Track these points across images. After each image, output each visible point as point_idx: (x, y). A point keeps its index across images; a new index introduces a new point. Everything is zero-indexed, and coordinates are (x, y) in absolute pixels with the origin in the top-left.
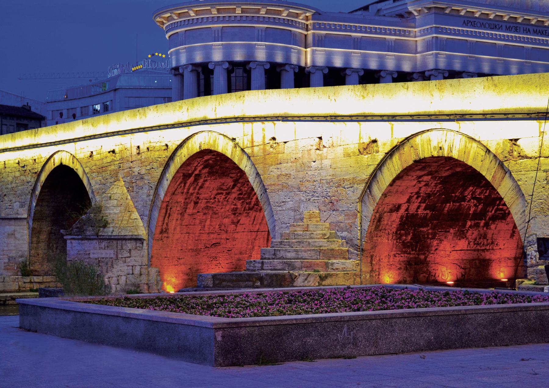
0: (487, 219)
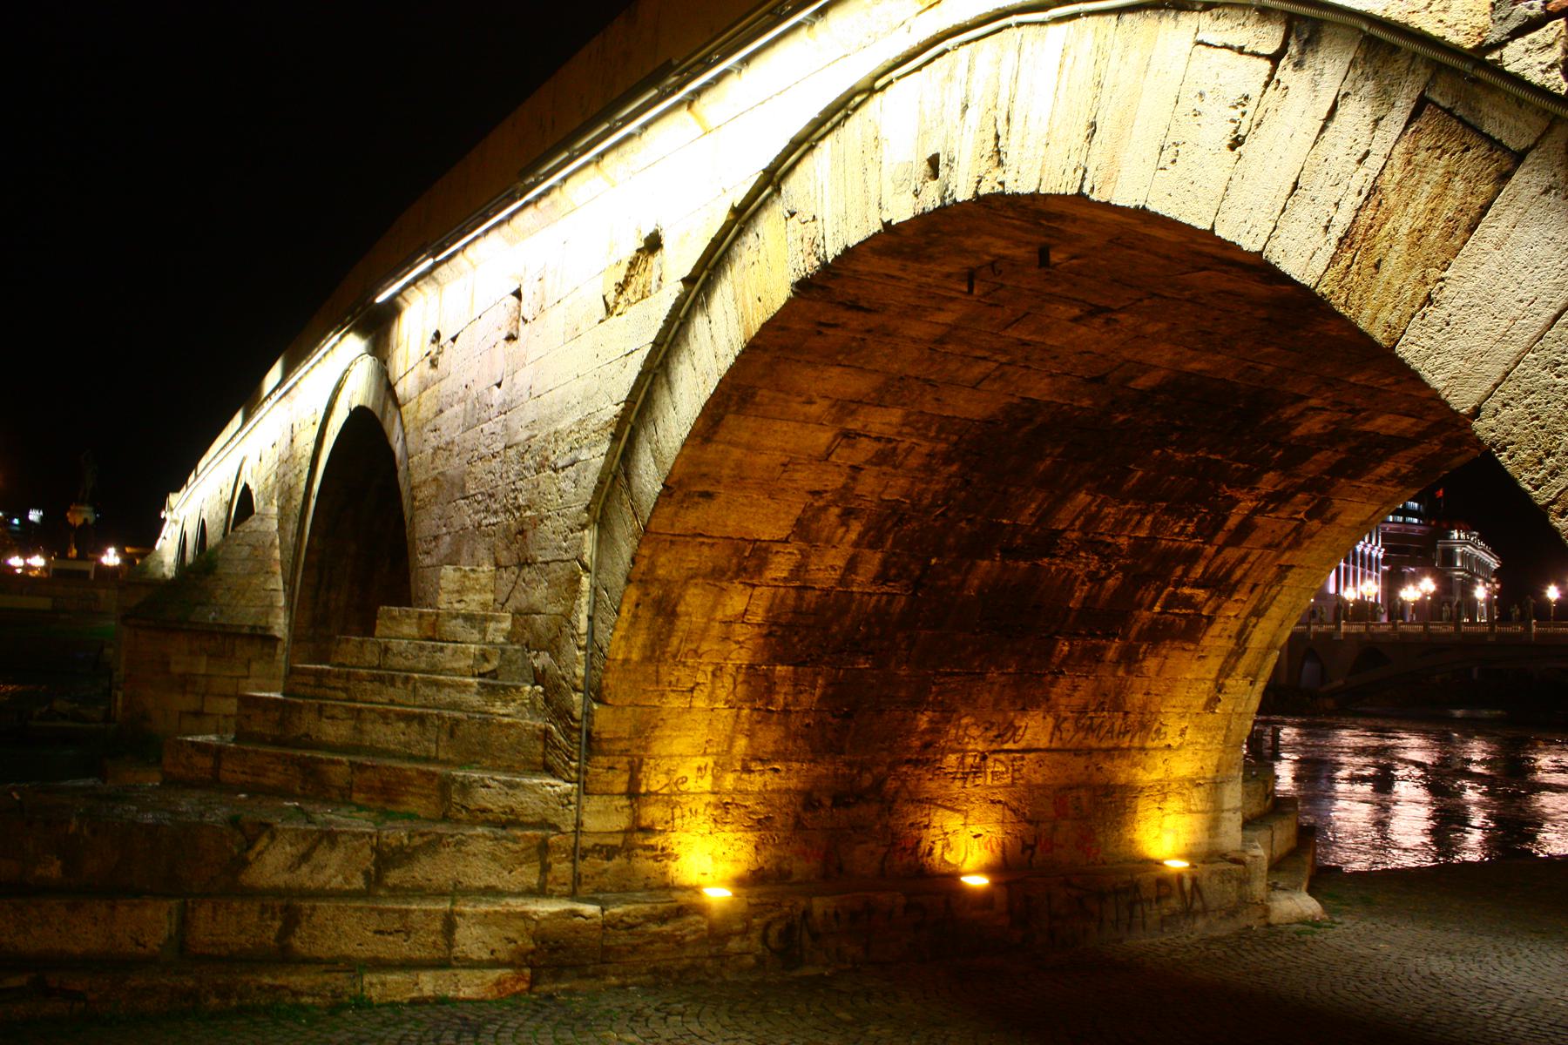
0: (1133, 634)
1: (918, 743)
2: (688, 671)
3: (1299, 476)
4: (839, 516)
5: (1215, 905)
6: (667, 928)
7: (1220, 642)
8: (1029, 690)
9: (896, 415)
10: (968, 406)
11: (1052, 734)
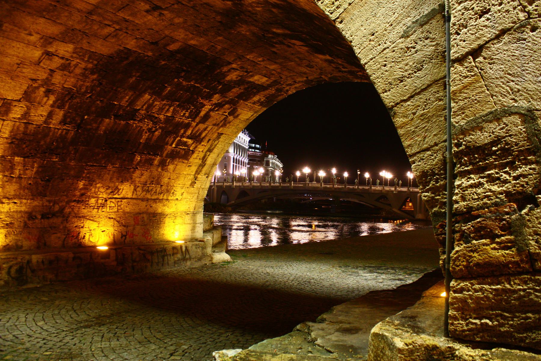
1: (79, 193)
3: (227, 97)
4: (44, 92)
7: (197, 161)
8: (124, 175)
9: (70, 47)
10: (102, 48)
11: (133, 192)
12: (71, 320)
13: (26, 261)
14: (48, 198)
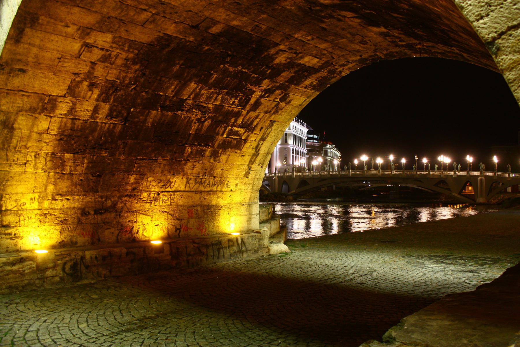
0: (216, 145)
1: (130, 188)
2: (22, 155)
3: (277, 82)
4: (88, 86)
5: (250, 248)
6: (15, 268)
8: (175, 167)
9: (109, 37)
10: (143, 36)
11: (186, 185)
12: (114, 321)
13: (79, 258)
14: (100, 194)
